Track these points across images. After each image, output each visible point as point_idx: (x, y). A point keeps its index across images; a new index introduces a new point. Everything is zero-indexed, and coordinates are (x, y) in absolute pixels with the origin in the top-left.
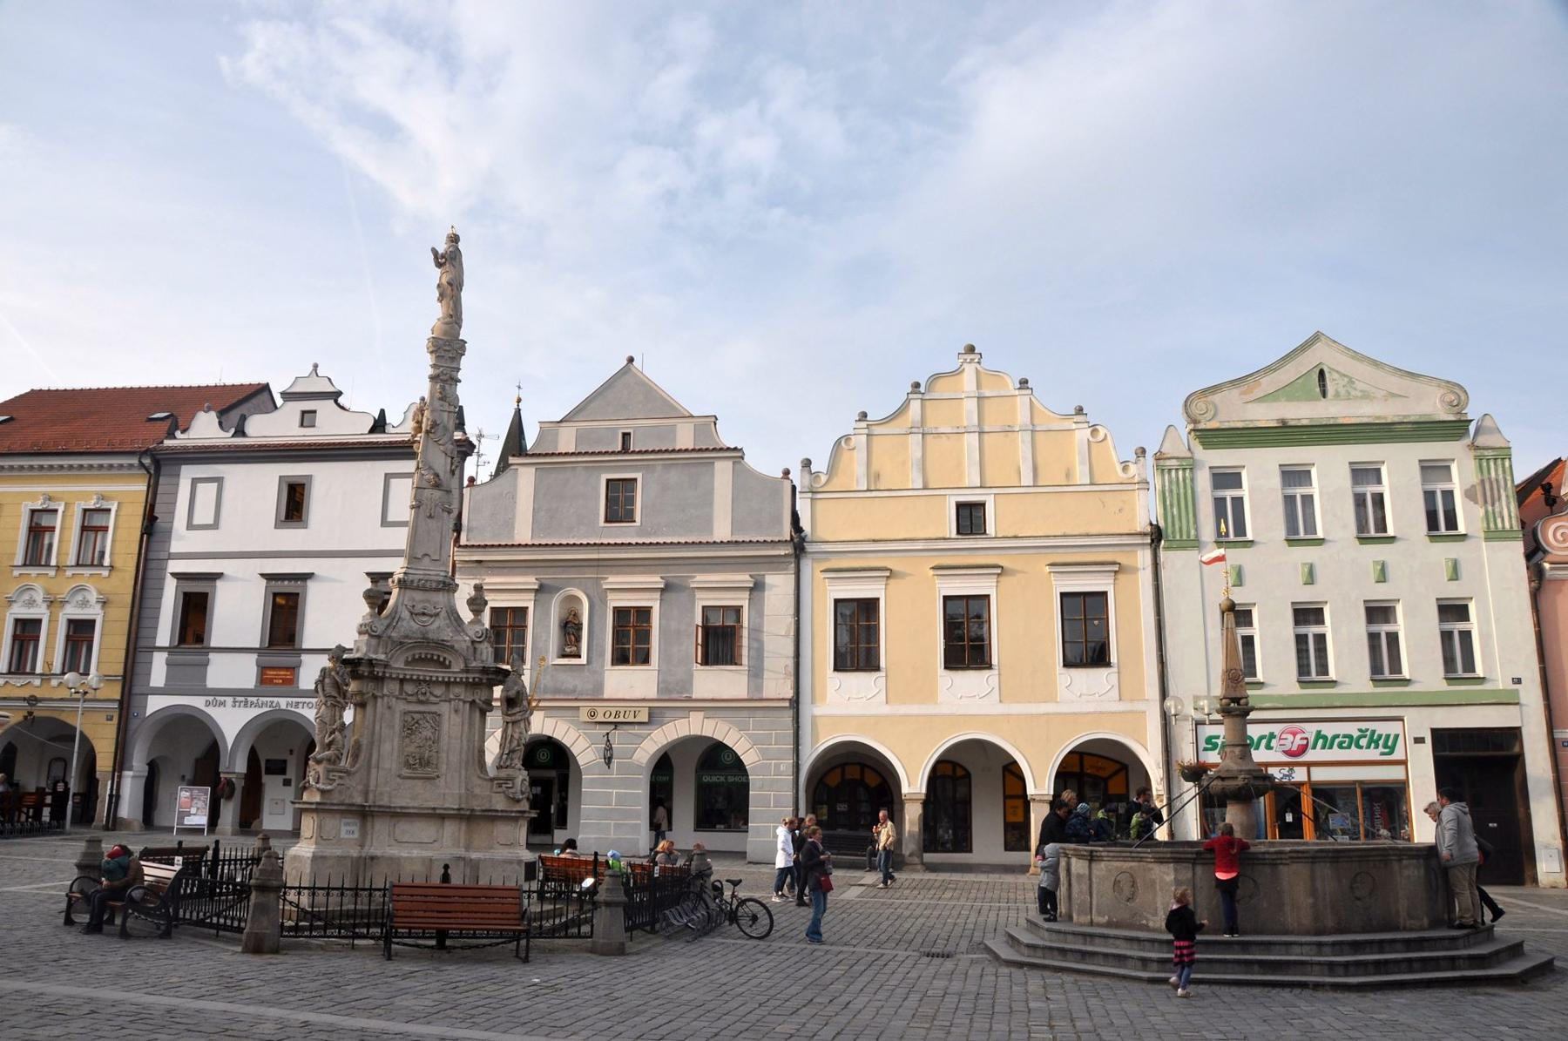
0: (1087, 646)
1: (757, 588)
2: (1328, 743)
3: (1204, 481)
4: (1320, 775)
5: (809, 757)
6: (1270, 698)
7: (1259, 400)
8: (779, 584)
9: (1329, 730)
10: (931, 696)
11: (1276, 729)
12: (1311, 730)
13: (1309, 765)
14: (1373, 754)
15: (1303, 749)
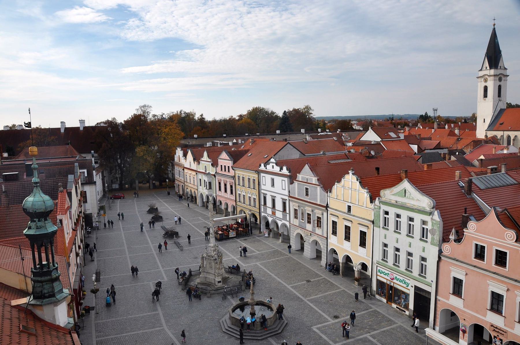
0: (363, 244)
1: (323, 214)
2: (397, 280)
3: (382, 213)
4: (396, 286)
5: (329, 249)
6: (388, 266)
7: (393, 195)
8: (325, 214)
9: (398, 277)
10: (342, 244)
11: (390, 273)
12: (395, 275)
13: (394, 283)
14: (405, 286)
15: (393, 279)
